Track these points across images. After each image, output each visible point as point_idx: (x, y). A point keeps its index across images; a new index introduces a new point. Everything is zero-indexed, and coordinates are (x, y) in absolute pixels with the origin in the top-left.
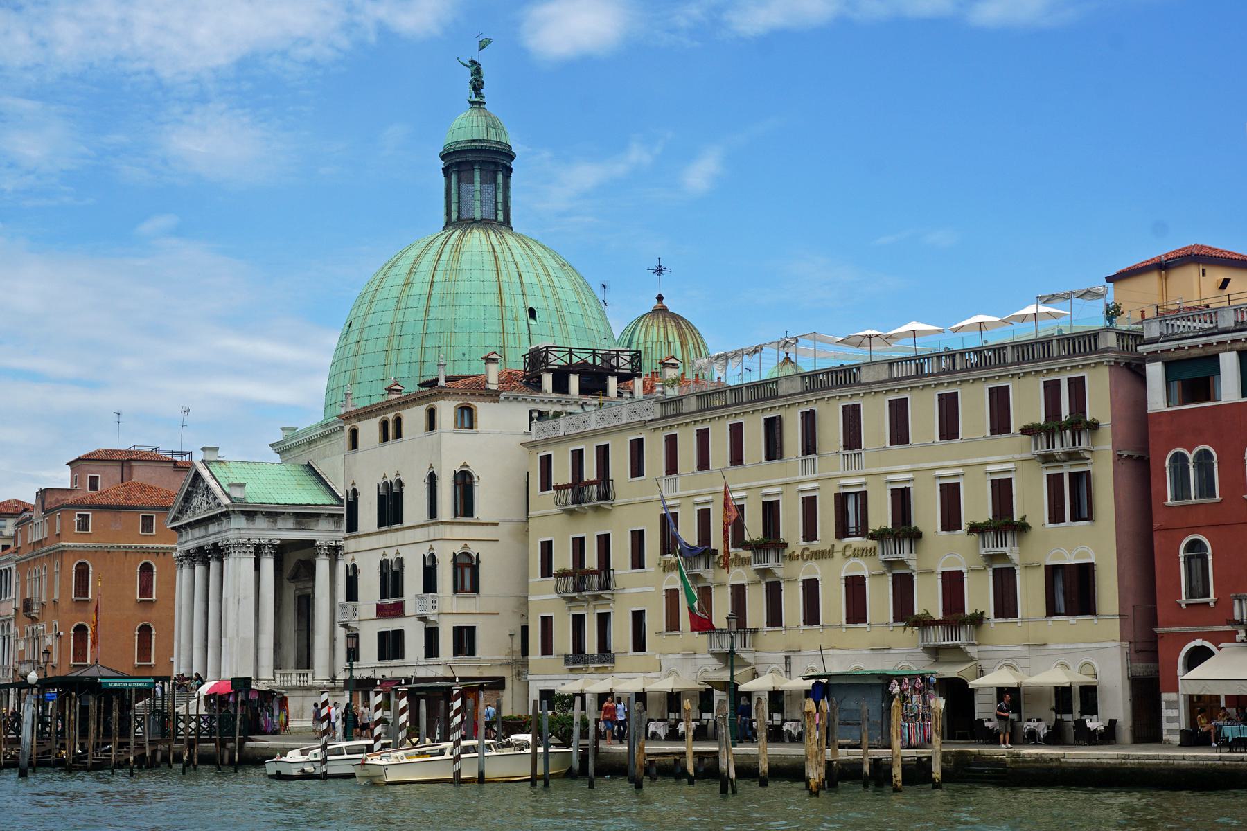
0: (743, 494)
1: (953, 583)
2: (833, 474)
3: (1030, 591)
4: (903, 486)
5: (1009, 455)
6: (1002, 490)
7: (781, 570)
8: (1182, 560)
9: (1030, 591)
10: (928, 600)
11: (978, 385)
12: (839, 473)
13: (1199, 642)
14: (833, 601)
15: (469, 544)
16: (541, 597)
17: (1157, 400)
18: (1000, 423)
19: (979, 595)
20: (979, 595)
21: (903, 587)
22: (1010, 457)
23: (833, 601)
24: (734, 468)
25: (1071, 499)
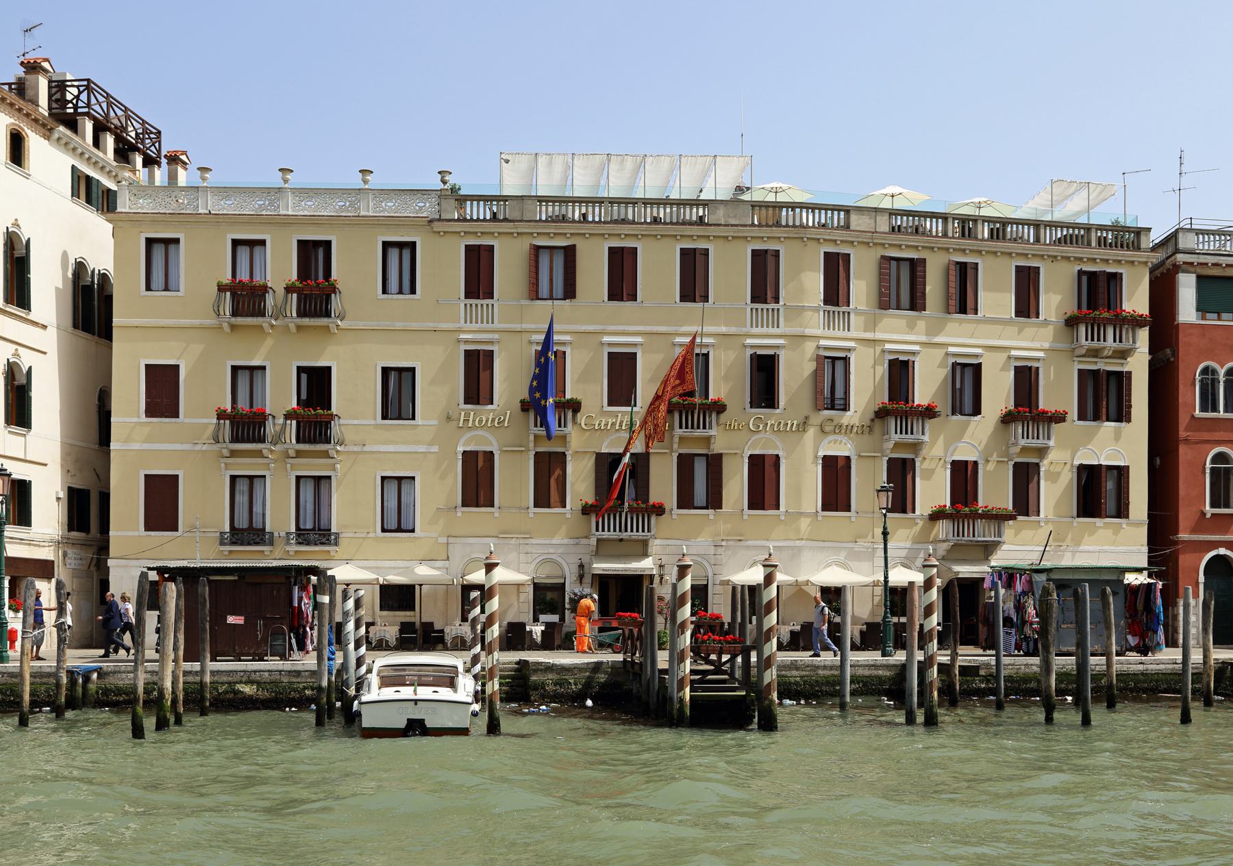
0: (567, 338)
1: (964, 477)
2: (808, 332)
3: (1056, 490)
4: (770, 352)
5: (1034, 342)
6: (1026, 379)
7: (720, 438)
8: (1208, 471)
9: (1056, 490)
10: (933, 490)
11: (1004, 261)
12: (819, 332)
13: (1222, 551)
14: (802, 483)
15: (21, 350)
16: (178, 447)
17: (1187, 309)
18: (1026, 306)
19: (995, 491)
20: (995, 491)
21: (901, 475)
22: (1038, 345)
23: (802, 483)
24: (616, 304)
25: (1103, 396)
